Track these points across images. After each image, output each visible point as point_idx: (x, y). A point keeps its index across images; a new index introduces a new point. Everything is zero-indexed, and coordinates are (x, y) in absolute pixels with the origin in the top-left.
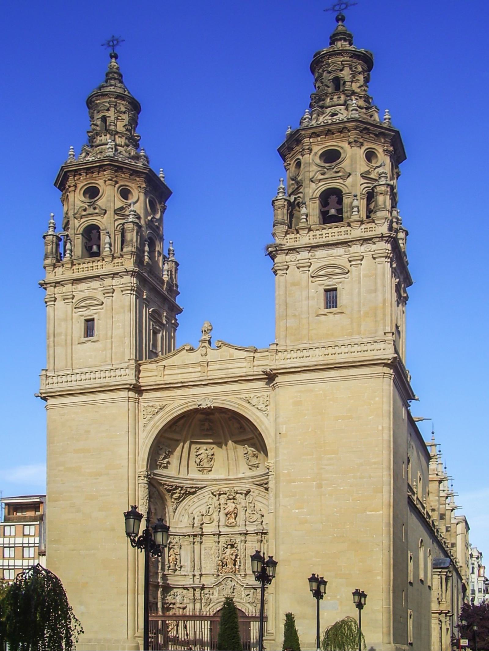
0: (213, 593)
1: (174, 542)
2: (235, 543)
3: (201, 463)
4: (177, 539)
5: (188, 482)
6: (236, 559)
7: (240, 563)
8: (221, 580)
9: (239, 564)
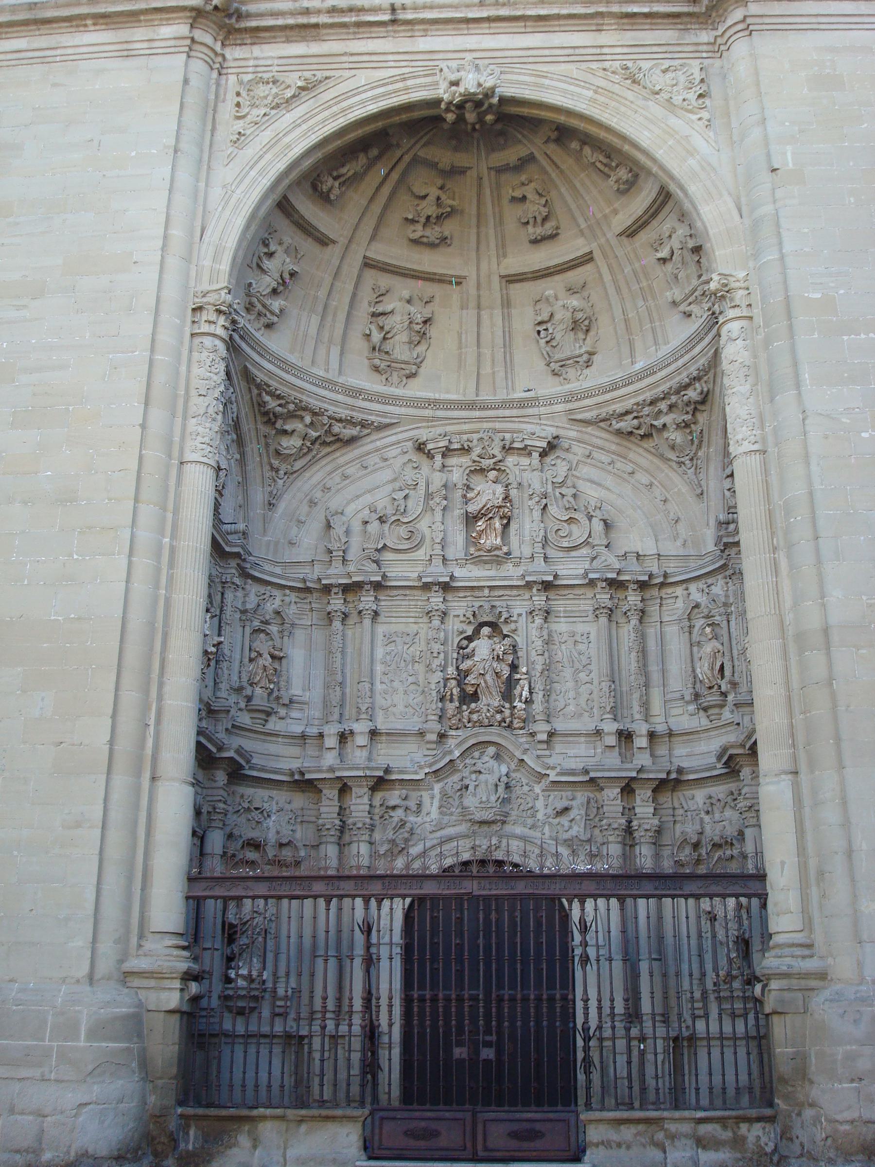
0: (419, 805)
1: (270, 607)
2: (506, 621)
3: (387, 346)
4: (277, 602)
5: (340, 398)
6: (518, 676)
7: (531, 693)
8: (457, 753)
9: (525, 693)
